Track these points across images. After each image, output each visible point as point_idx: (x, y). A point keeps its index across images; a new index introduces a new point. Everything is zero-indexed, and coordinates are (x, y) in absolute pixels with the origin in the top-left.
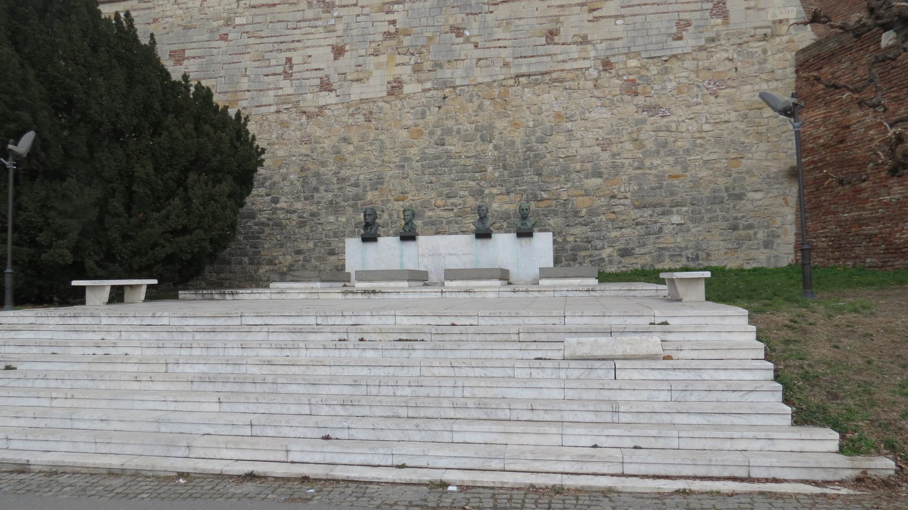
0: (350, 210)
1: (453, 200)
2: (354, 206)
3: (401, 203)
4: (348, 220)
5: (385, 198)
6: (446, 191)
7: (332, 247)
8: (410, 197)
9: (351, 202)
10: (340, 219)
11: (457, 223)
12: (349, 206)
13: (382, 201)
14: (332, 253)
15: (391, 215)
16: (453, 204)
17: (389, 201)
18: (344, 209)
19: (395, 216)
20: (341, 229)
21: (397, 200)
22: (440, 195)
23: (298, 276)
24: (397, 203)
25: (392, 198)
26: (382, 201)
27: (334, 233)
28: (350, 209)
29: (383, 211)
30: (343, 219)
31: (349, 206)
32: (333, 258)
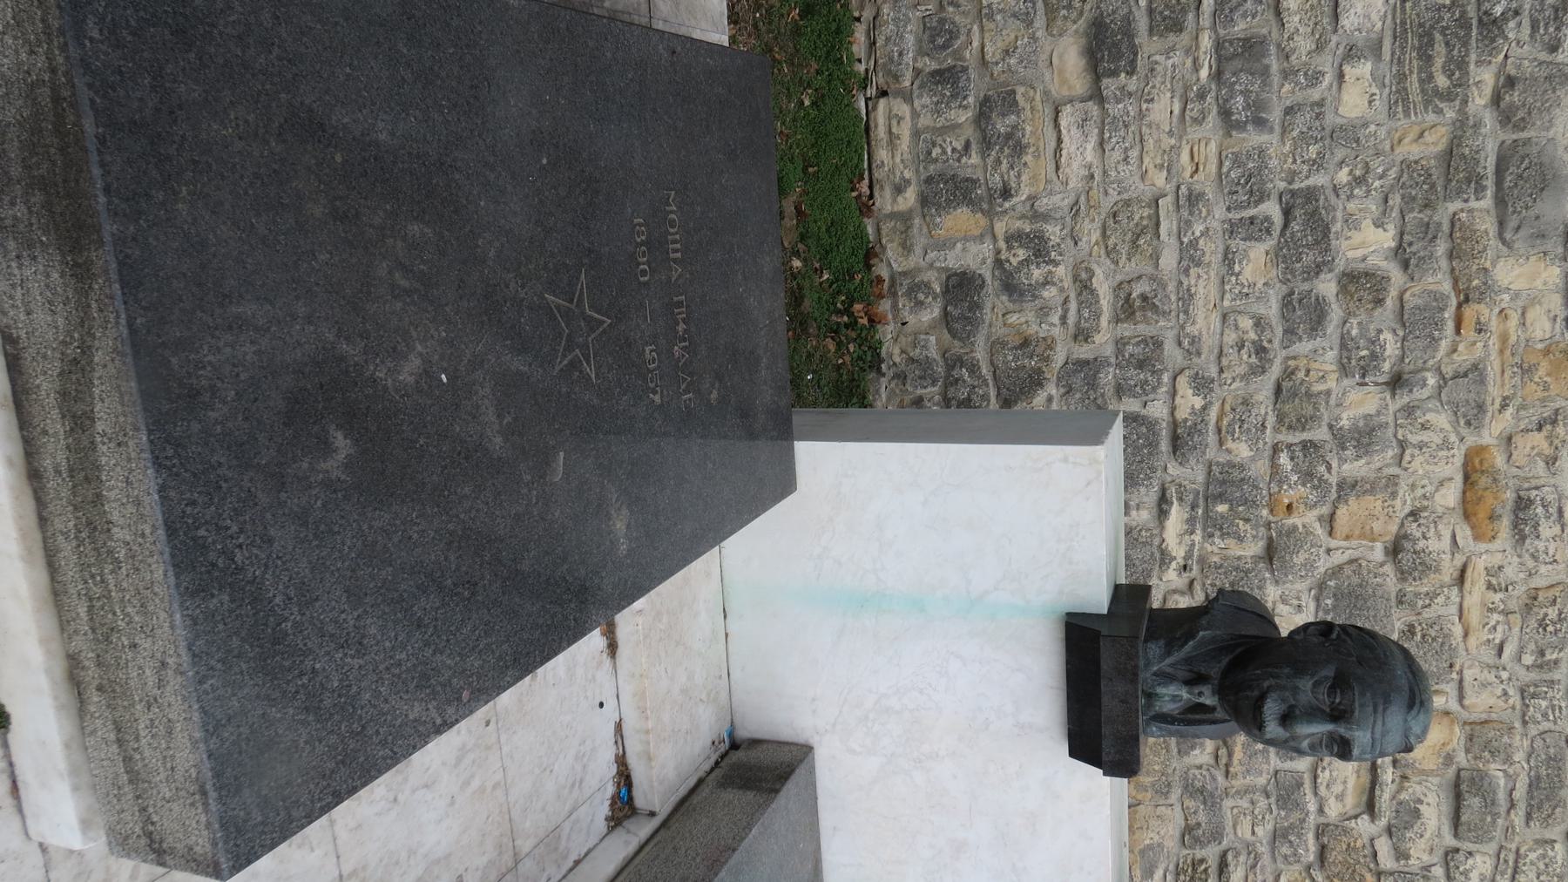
0: (1425, 140)
1: (1434, 815)
2: (1455, 167)
3: (1450, 496)
4: (1349, 134)
5: (1494, 392)
6: (1509, 776)
7: (1148, 45)
8: (1494, 553)
9: (1489, 141)
10: (1362, 70)
11: (1278, 836)
12: (1463, 126)
13: (1475, 371)
14: (1107, 49)
15: (1363, 437)
16: (1410, 814)
17: (1474, 415)
18: (1433, 97)
19: (1355, 468)
20: (1283, 94)
21: (1471, 472)
22: (1479, 735)
23: (85, 471)
24: (1452, 468)
25: (1489, 435)
26: (1475, 371)
27: (1252, 47)
28: (1437, 141)
29: (1396, 382)
30: (1357, 96)
31: (1463, 126)
32: (1069, 56)
